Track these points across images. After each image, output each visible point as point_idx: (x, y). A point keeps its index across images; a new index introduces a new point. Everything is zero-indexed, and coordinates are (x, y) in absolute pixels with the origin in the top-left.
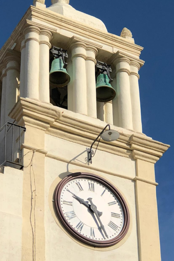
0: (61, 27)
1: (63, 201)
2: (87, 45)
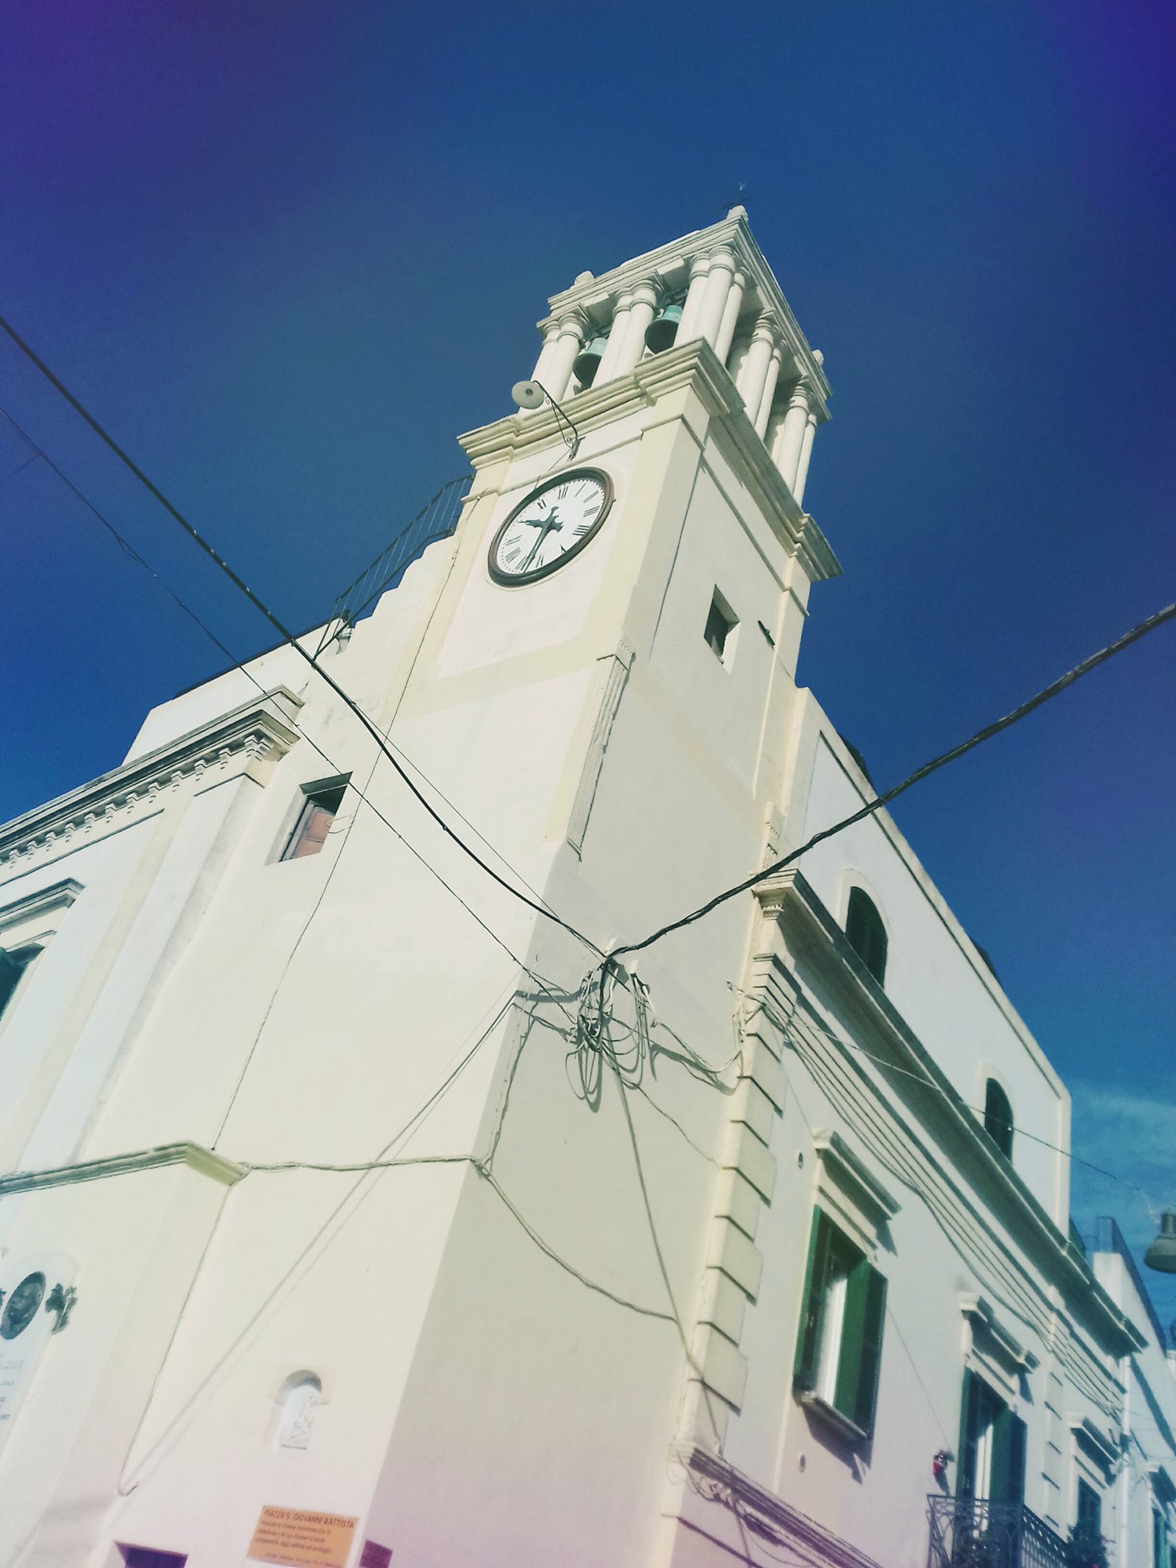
0: (596, 293)
2: (629, 287)
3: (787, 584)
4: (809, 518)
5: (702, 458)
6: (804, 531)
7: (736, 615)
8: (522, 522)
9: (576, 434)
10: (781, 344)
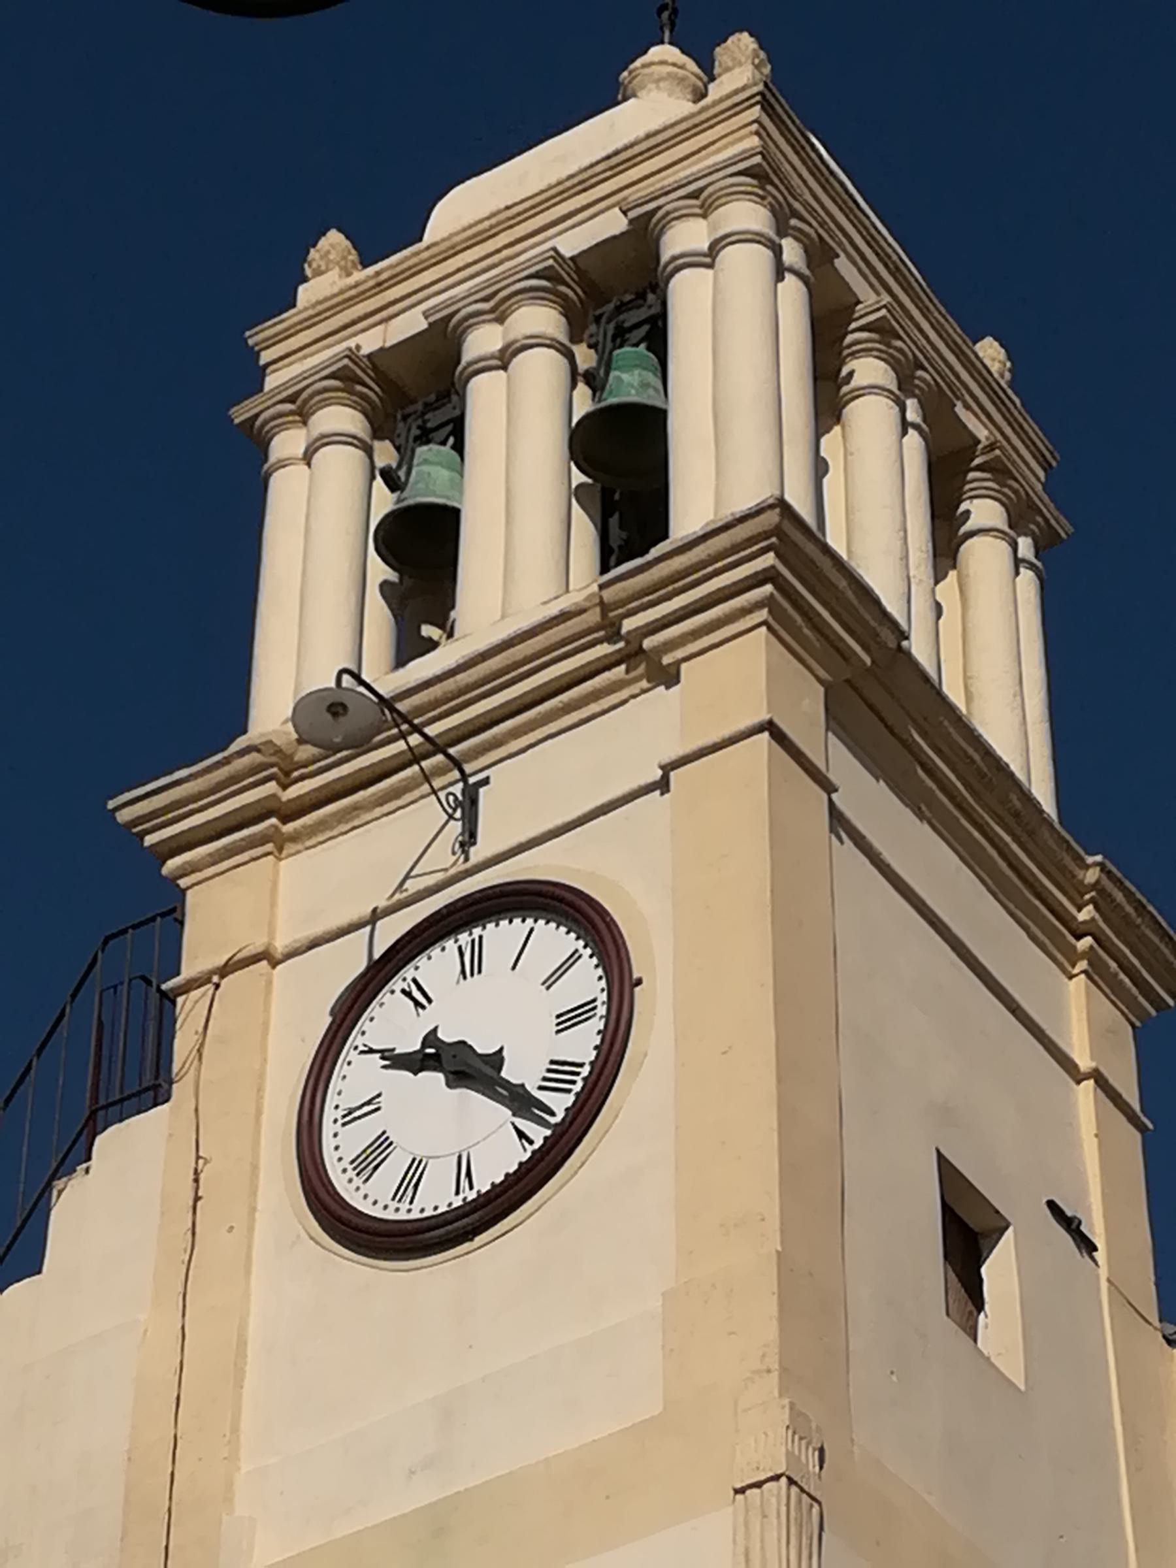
0: (383, 315)
1: (344, 1116)
3: (1085, 1063)
4: (1102, 866)
5: (835, 815)
6: (1092, 901)
7: (997, 1212)
8: (371, 1051)
9: (462, 771)
10: (917, 382)
